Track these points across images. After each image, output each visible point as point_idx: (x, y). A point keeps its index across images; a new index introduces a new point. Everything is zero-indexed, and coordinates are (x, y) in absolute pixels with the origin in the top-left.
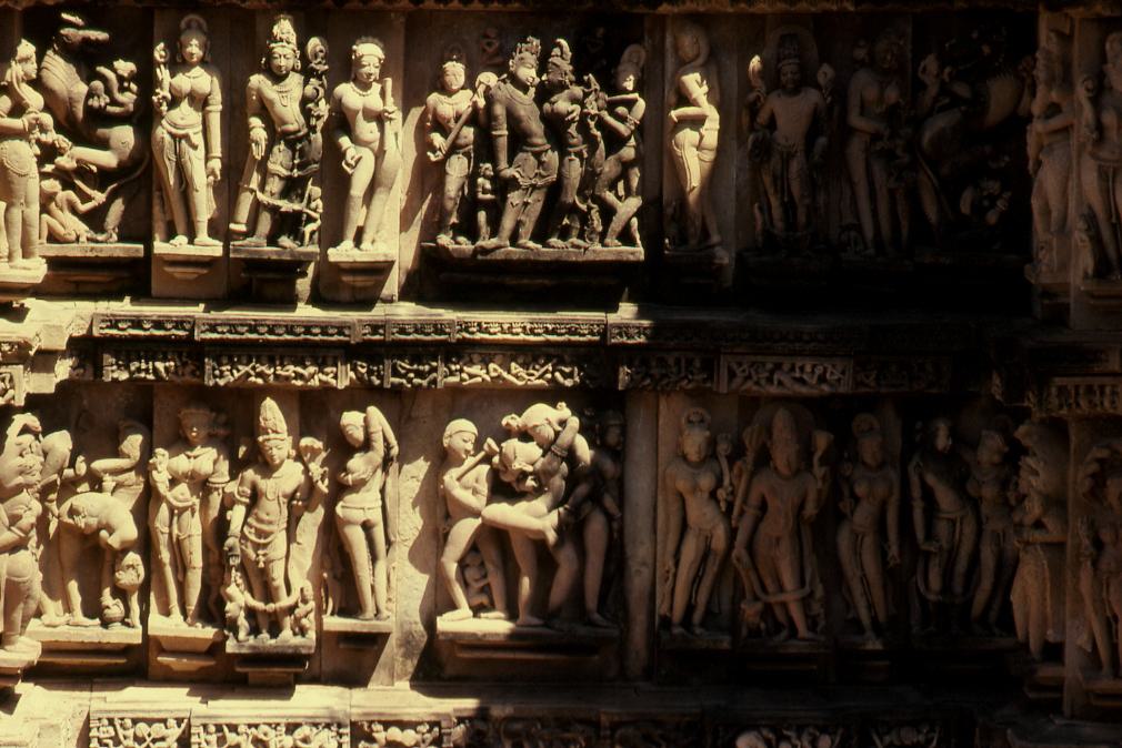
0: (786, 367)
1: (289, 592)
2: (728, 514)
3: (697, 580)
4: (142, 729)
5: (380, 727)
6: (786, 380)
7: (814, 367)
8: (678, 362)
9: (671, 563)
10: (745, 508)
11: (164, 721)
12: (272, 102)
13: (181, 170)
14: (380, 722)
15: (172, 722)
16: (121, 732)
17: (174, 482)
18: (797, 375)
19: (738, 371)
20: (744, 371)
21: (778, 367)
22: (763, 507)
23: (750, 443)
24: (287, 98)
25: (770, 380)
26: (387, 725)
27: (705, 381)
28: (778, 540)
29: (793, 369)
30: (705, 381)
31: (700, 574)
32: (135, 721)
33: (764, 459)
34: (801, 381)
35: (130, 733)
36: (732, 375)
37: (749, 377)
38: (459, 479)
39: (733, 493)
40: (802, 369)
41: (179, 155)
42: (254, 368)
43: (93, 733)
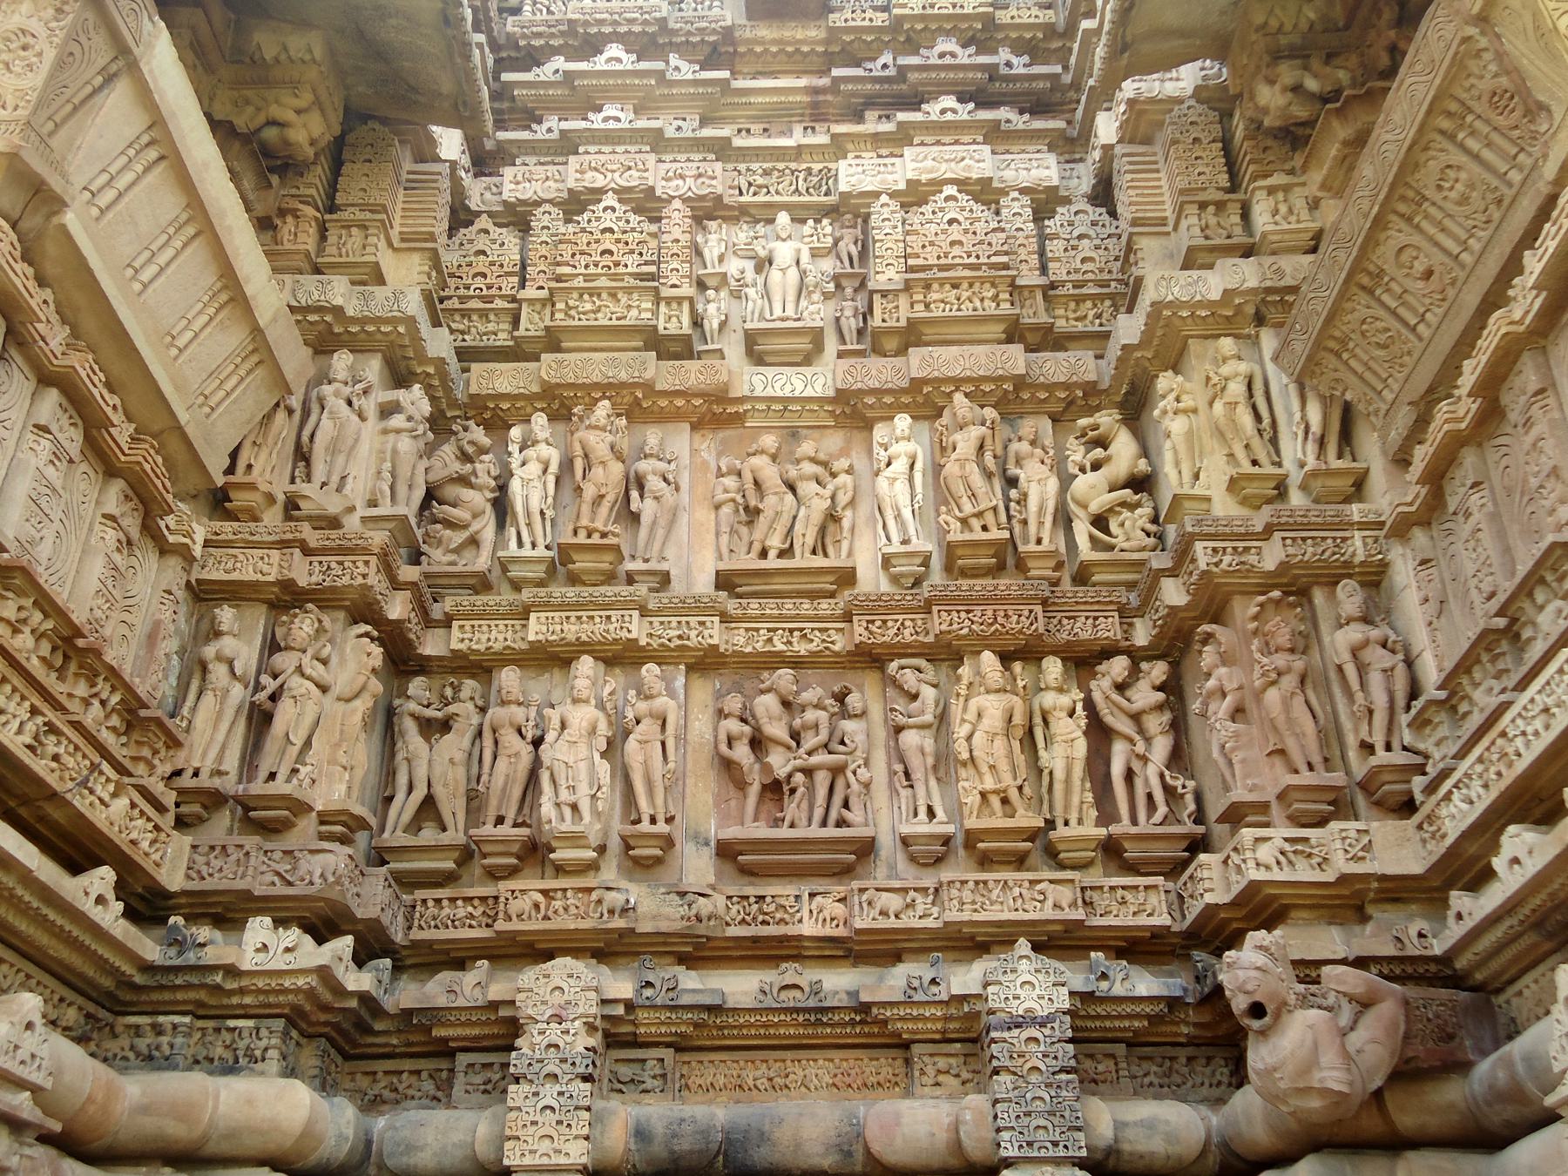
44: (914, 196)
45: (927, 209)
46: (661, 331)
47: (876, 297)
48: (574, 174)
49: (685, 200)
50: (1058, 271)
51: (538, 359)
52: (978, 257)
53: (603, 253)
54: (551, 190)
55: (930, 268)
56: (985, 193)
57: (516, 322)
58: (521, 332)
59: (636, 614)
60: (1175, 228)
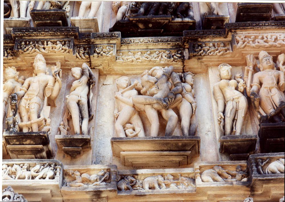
0: (260, 37)
1: (39, 117)
5: (78, 174)
6: (261, 41)
7: (271, 36)
9: (222, 114)
10: (252, 84)
18: (265, 39)
20: (242, 39)
21: (256, 38)
22: (261, 84)
23: (250, 59)
31: (236, 118)
37: (244, 42)
38: (122, 93)
40: (267, 37)
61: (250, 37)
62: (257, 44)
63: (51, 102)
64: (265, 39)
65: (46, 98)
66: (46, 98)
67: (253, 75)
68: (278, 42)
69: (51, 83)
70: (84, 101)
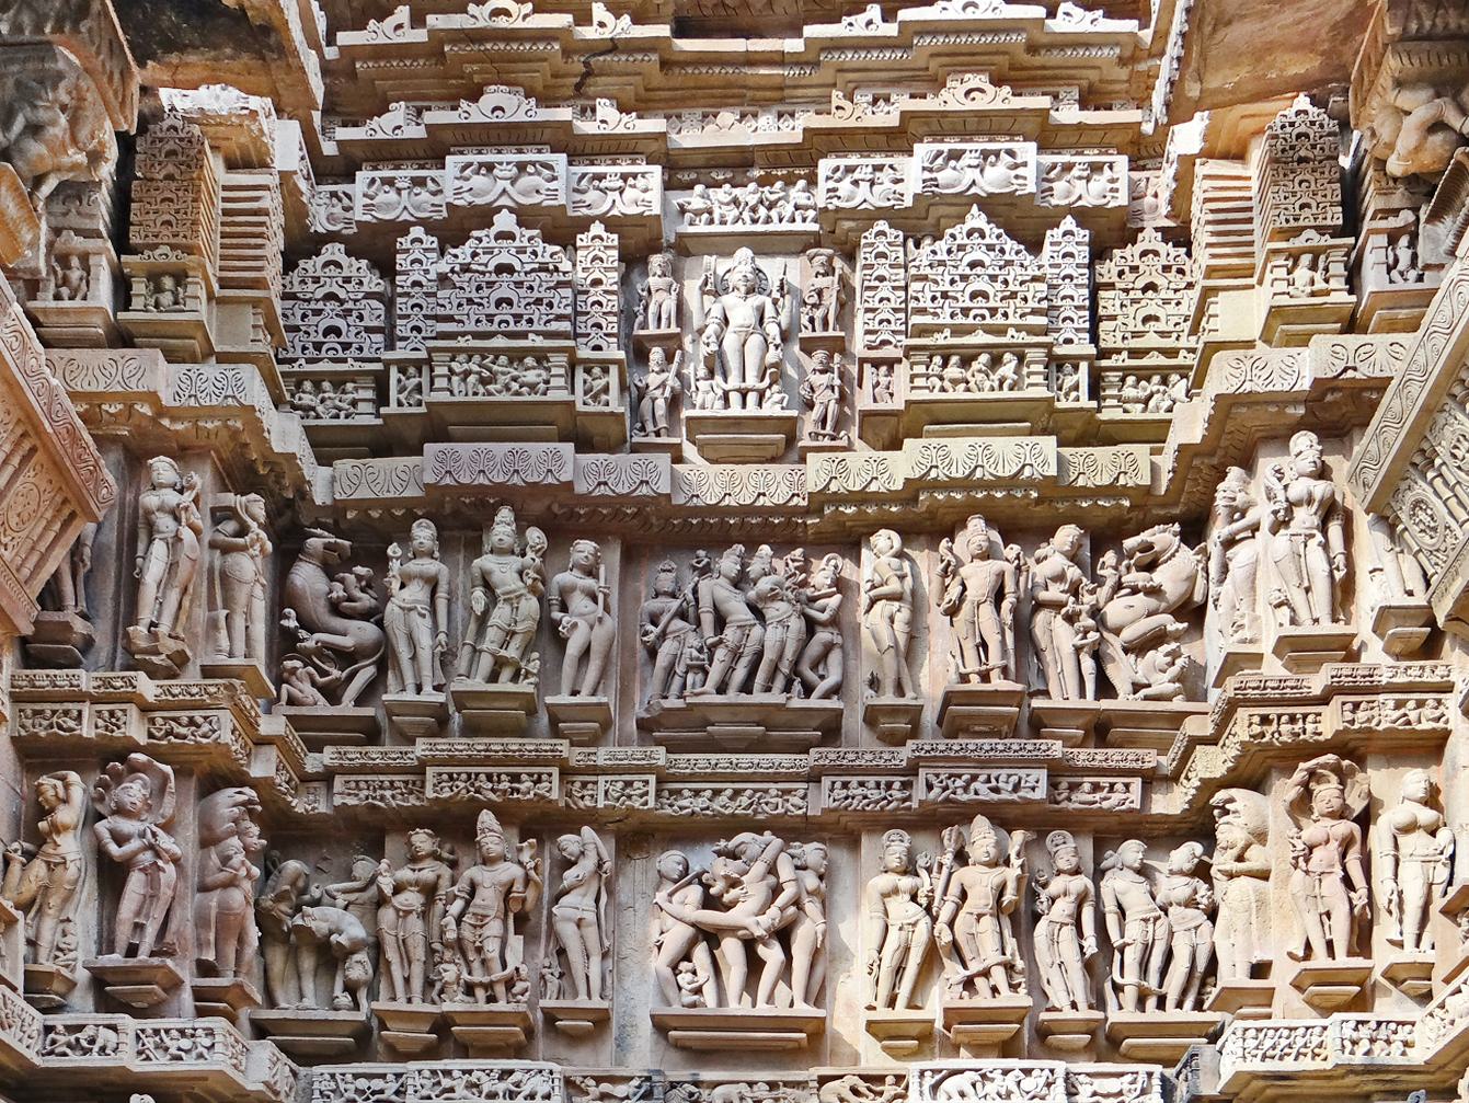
1: (504, 966)
2: (928, 909)
3: (899, 970)
4: (362, 1083)
5: (593, 1083)
8: (878, 785)
11: (383, 1076)
12: (490, 573)
13: (411, 638)
14: (593, 1078)
15: (390, 1077)
16: (342, 1086)
17: (398, 889)
18: (994, 783)
19: (935, 782)
21: (974, 778)
22: (964, 896)
24: (504, 571)
25: (966, 789)
26: (599, 1080)
27: (904, 800)
28: (979, 916)
29: (988, 781)
30: (904, 800)
32: (356, 1076)
33: (961, 858)
34: (996, 790)
35: (352, 1087)
36: (930, 787)
37: (946, 788)
39: (932, 891)
41: (407, 624)
42: (473, 785)
43: (316, 1085)
44: (921, 221)
45: (942, 246)
46: (580, 407)
47: (867, 367)
48: (458, 181)
49: (611, 224)
50: (1110, 336)
51: (420, 452)
52: (1005, 315)
53: (499, 303)
54: (423, 203)
55: (939, 329)
56: (1023, 222)
57: (382, 398)
58: (393, 408)
59: (555, 771)
60: (1260, 282)
61: (960, 776)
62: (971, 796)
63: (522, 922)
64: (994, 783)
65: (511, 916)
66: (511, 916)
67: (950, 874)
68: (1021, 794)
69: (518, 886)
70: (590, 917)
